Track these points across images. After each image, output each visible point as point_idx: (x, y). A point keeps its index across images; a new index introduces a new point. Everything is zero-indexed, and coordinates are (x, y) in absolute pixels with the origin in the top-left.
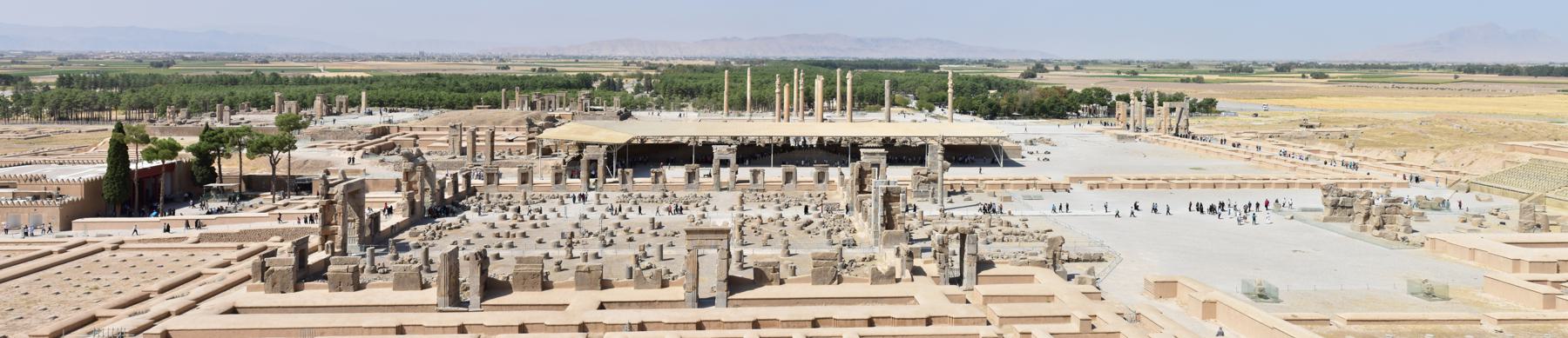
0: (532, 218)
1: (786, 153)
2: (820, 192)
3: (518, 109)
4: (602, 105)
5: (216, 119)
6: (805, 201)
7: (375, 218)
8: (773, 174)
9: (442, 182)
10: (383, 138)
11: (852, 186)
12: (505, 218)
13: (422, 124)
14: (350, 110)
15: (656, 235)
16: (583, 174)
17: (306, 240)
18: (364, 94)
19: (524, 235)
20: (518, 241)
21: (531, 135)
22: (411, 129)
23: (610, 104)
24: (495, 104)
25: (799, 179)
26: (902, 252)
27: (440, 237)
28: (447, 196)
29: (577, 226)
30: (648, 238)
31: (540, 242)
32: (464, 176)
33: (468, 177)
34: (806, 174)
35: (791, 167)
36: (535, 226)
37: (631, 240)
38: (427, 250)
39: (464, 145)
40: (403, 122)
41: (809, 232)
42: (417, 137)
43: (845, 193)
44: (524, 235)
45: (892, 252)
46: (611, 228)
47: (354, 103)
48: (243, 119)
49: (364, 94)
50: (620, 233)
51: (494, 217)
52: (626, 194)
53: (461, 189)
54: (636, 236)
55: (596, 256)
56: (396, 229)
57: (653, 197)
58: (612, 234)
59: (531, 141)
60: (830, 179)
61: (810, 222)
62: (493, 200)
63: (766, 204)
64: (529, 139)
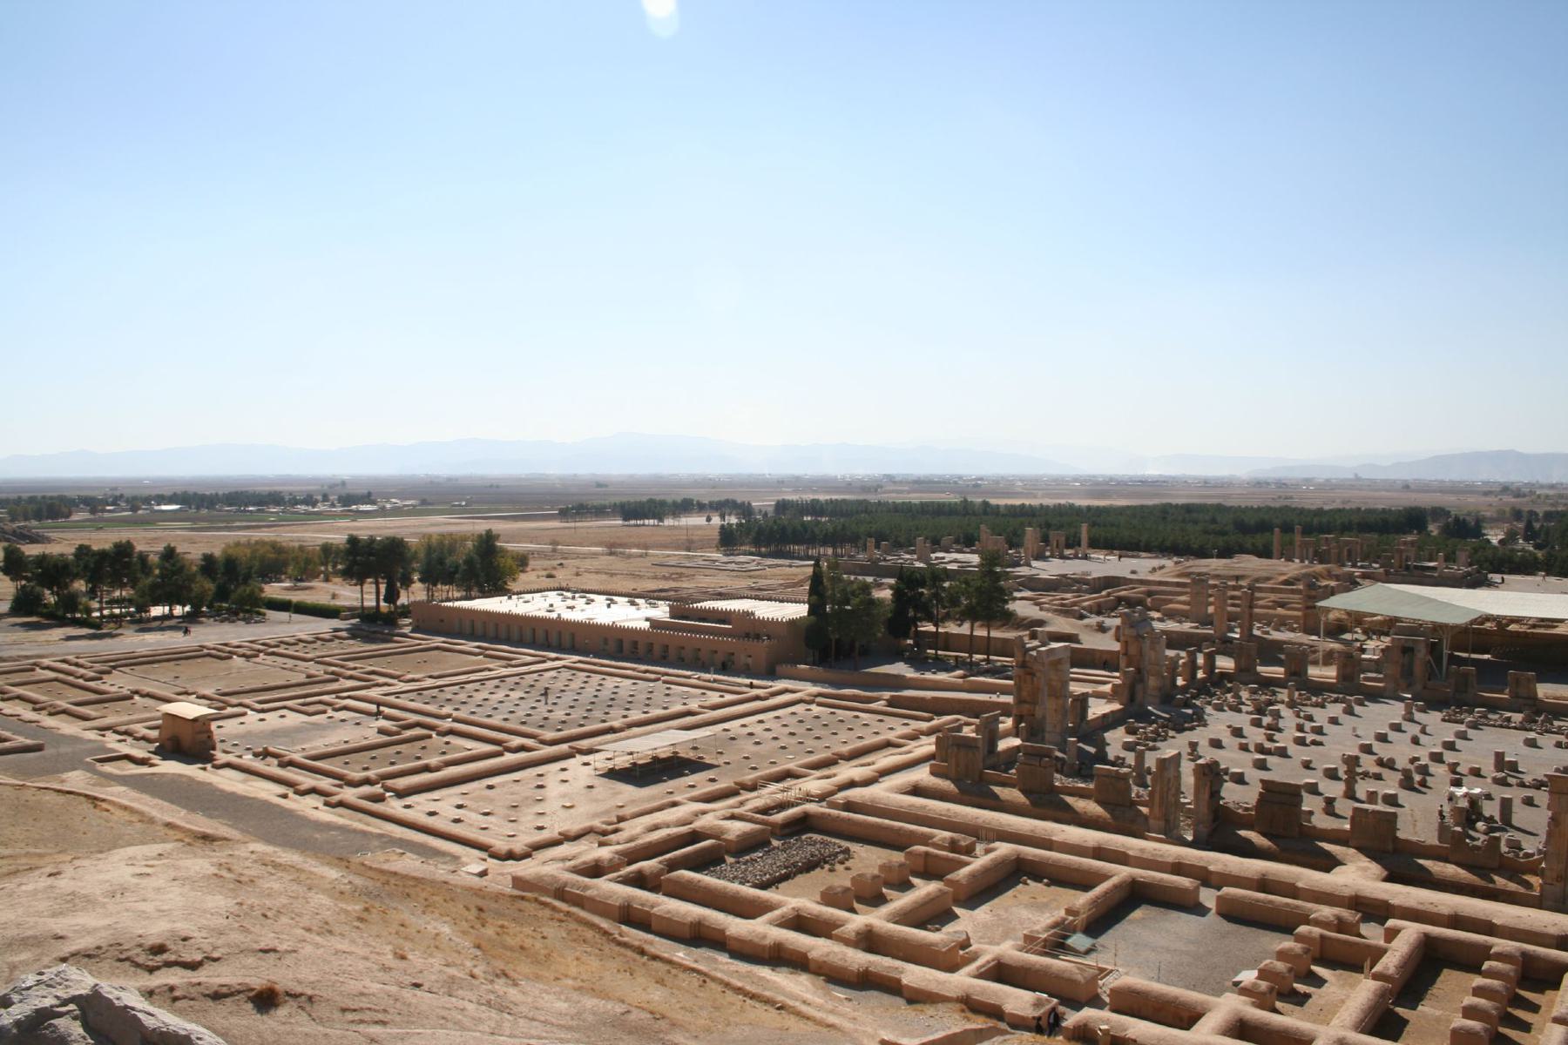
3: (1297, 561)
5: (915, 557)
7: (1082, 701)
9: (1174, 661)
10: (1104, 593)
12: (1257, 723)
13: (1156, 577)
14: (1068, 552)
17: (996, 720)
18: (1084, 528)
19: (1282, 753)
20: (1272, 760)
22: (1142, 582)
23: (1450, 558)
24: (1265, 553)
27: (1165, 740)
28: (1180, 682)
29: (1367, 749)
31: (1307, 765)
32: (1206, 654)
33: (1210, 659)
36: (1300, 742)
38: (1142, 752)
39: (1211, 609)
40: (1133, 572)
42: (1150, 594)
44: (1282, 753)
46: (1425, 761)
47: (1073, 543)
48: (943, 558)
49: (1084, 528)
50: (1439, 770)
51: (1242, 720)
53: (1200, 674)
55: (1391, 800)
56: (1109, 722)
58: (1424, 770)
59: (1309, 611)
62: (1244, 695)
64: (1308, 608)
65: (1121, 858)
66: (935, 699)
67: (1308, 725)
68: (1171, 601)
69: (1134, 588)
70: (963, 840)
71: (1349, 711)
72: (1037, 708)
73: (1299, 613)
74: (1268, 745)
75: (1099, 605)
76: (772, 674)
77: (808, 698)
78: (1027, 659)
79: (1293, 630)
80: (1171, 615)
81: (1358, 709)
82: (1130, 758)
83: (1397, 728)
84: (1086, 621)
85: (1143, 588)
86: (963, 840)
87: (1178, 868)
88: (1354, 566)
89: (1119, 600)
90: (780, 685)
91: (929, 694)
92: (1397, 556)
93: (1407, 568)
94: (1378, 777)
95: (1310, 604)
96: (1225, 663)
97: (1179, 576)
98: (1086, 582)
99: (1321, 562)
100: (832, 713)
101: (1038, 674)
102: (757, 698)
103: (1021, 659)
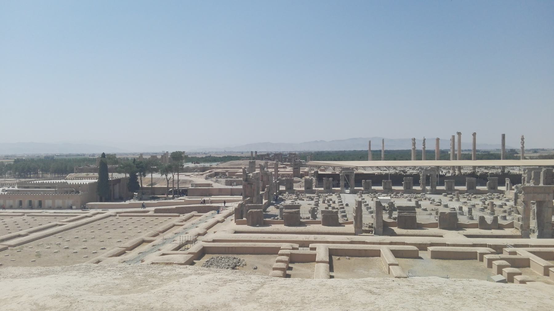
66: (176, 208)
68: (237, 172)
70: (296, 246)
72: (254, 198)
76: (84, 207)
77: (114, 214)
78: (248, 177)
86: (296, 246)
89: (216, 174)
90: (92, 211)
91: (174, 207)
95: (296, 167)
100: (130, 218)
101: (254, 184)
102: (87, 217)
103: (245, 178)
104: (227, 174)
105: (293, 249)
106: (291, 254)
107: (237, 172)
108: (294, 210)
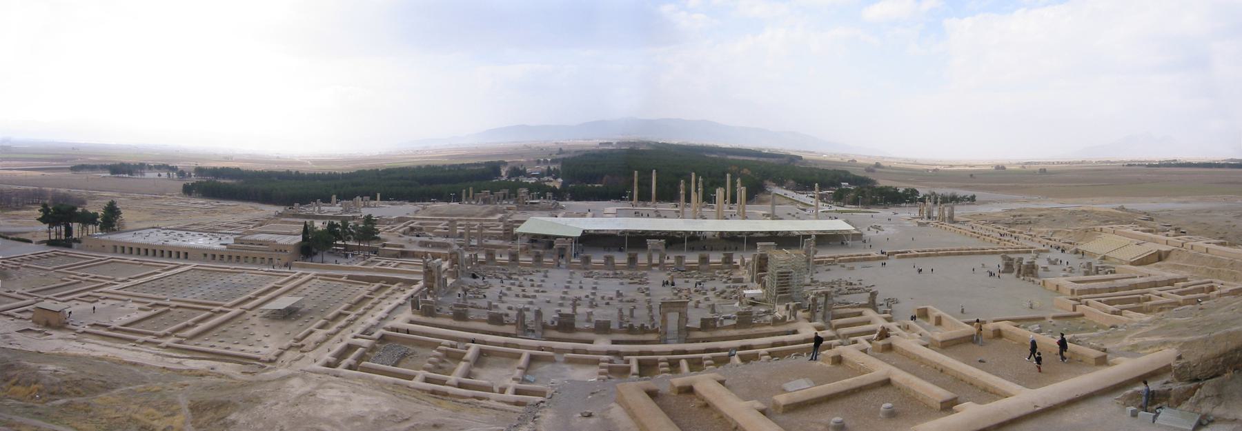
0: (532, 286)
1: (694, 241)
2: (726, 271)
4: (539, 198)
6: (717, 277)
7: (445, 280)
8: (692, 258)
11: (753, 268)
12: (513, 284)
15: (621, 301)
16: (556, 257)
21: (506, 228)
25: (710, 261)
26: (790, 307)
30: (615, 302)
33: (476, 255)
34: (716, 258)
35: (705, 253)
37: (608, 304)
39: (458, 231)
41: (725, 298)
42: (421, 224)
43: (747, 271)
45: (783, 307)
50: (598, 299)
52: (588, 272)
54: (611, 302)
55: (591, 314)
57: (608, 274)
60: (734, 260)
61: (722, 292)
63: (690, 280)
65: (518, 346)
67: (535, 285)
68: (436, 228)
69: (413, 223)
71: (546, 277)
73: (501, 232)
74: (527, 294)
75: (405, 231)
79: (497, 239)
80: (438, 235)
81: (548, 274)
82: (483, 303)
83: (570, 282)
84: (403, 239)
85: (417, 222)
87: (540, 348)
88: (501, 204)
89: (412, 229)
92: (521, 199)
93: (527, 203)
94: (579, 305)
96: (482, 257)
97: (432, 215)
98: (392, 220)
99: (485, 203)
104: (424, 227)
105: (452, 346)
106: (447, 351)
107: (436, 228)
108: (461, 309)
